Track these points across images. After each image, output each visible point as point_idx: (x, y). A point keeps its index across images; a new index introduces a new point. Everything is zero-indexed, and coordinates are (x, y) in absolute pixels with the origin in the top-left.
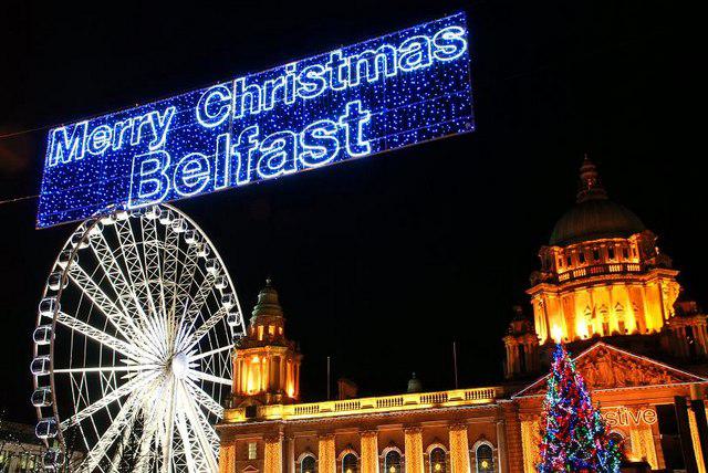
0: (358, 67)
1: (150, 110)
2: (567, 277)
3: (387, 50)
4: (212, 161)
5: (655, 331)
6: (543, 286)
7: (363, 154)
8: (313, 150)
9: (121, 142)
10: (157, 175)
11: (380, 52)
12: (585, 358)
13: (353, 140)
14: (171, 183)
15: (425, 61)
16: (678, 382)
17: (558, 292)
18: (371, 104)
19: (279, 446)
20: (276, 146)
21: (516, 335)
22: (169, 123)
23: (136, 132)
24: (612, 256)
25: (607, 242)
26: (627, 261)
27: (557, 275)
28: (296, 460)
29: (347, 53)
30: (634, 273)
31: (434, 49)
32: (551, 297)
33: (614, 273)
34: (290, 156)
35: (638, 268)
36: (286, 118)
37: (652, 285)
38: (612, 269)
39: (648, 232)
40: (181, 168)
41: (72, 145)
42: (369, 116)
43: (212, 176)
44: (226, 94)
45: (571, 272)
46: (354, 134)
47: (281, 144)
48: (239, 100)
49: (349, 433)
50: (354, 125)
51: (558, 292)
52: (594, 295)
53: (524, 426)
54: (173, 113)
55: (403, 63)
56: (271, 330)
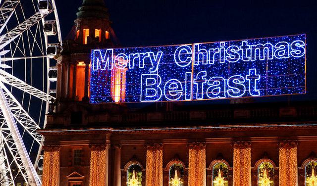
0: (255, 51)
1: (149, 51)
3: (269, 46)
4: (183, 84)
8: (234, 89)
9: (133, 65)
10: (155, 87)
11: (266, 46)
13: (252, 88)
15: (286, 55)
18: (261, 71)
19: (104, 155)
20: (215, 83)
23: (142, 61)
28: (122, 167)
29: (251, 43)
31: (290, 50)
34: (222, 89)
40: (168, 85)
41: (106, 60)
42: (260, 77)
43: (184, 93)
44: (189, 51)
46: (253, 85)
47: (218, 83)
48: (196, 55)
49: (178, 143)
50: (253, 81)
54: (161, 55)
55: (277, 53)
56: (97, 33)
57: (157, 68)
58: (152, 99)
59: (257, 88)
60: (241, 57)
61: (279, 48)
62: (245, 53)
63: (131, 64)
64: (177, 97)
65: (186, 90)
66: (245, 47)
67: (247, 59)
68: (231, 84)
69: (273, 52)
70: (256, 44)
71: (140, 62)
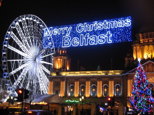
0: (110, 24)
1: (66, 27)
2: (142, 42)
3: (115, 22)
6: (136, 44)
7: (110, 43)
9: (60, 33)
10: (68, 41)
11: (114, 22)
12: (146, 64)
13: (108, 40)
14: (71, 43)
17: (140, 46)
18: (112, 32)
19: (64, 83)
20: (93, 38)
21: (128, 57)
22: (70, 30)
23: (63, 31)
27: (140, 42)
28: (69, 86)
31: (124, 23)
36: (95, 33)
43: (80, 43)
44: (82, 26)
46: (108, 38)
47: (94, 38)
48: (85, 28)
49: (83, 80)
51: (140, 46)
52: (149, 47)
53: (129, 81)
54: (71, 28)
56: (63, 52)
57: (69, 34)
58: (67, 46)
59: (110, 40)
60: (103, 27)
61: (119, 23)
62: (105, 25)
63: (59, 33)
64: (77, 45)
65: (81, 42)
66: (105, 23)
67: (106, 28)
68: (99, 38)
69: (117, 24)
70: (110, 22)
71: (63, 31)
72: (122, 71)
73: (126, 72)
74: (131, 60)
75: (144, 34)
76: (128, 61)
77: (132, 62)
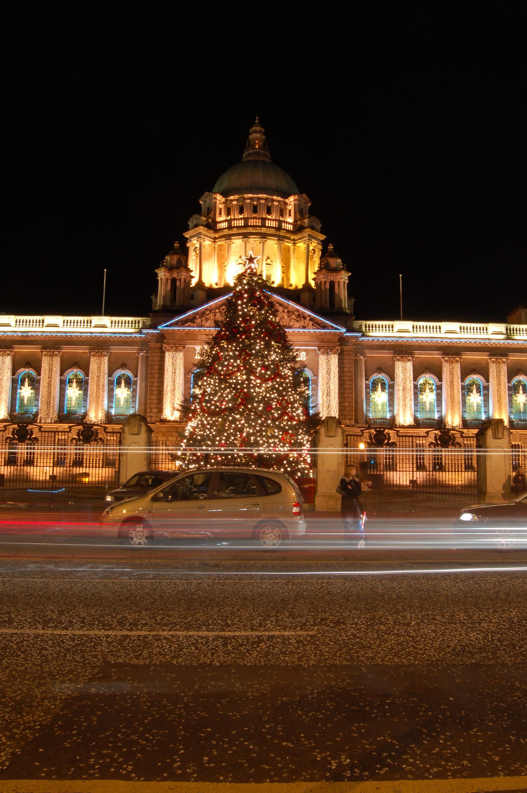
5: (296, 287)
16: (319, 329)
17: (215, 238)
21: (171, 269)
24: (269, 212)
25: (266, 199)
26: (282, 219)
27: (215, 223)
30: (288, 231)
32: (207, 243)
33: (271, 227)
35: (290, 227)
37: (301, 245)
38: (268, 223)
39: (304, 195)
45: (230, 221)
53: (168, 356)
72: (144, 322)
73: (160, 324)
74: (180, 280)
75: (232, 197)
76: (169, 281)
77: (182, 286)
